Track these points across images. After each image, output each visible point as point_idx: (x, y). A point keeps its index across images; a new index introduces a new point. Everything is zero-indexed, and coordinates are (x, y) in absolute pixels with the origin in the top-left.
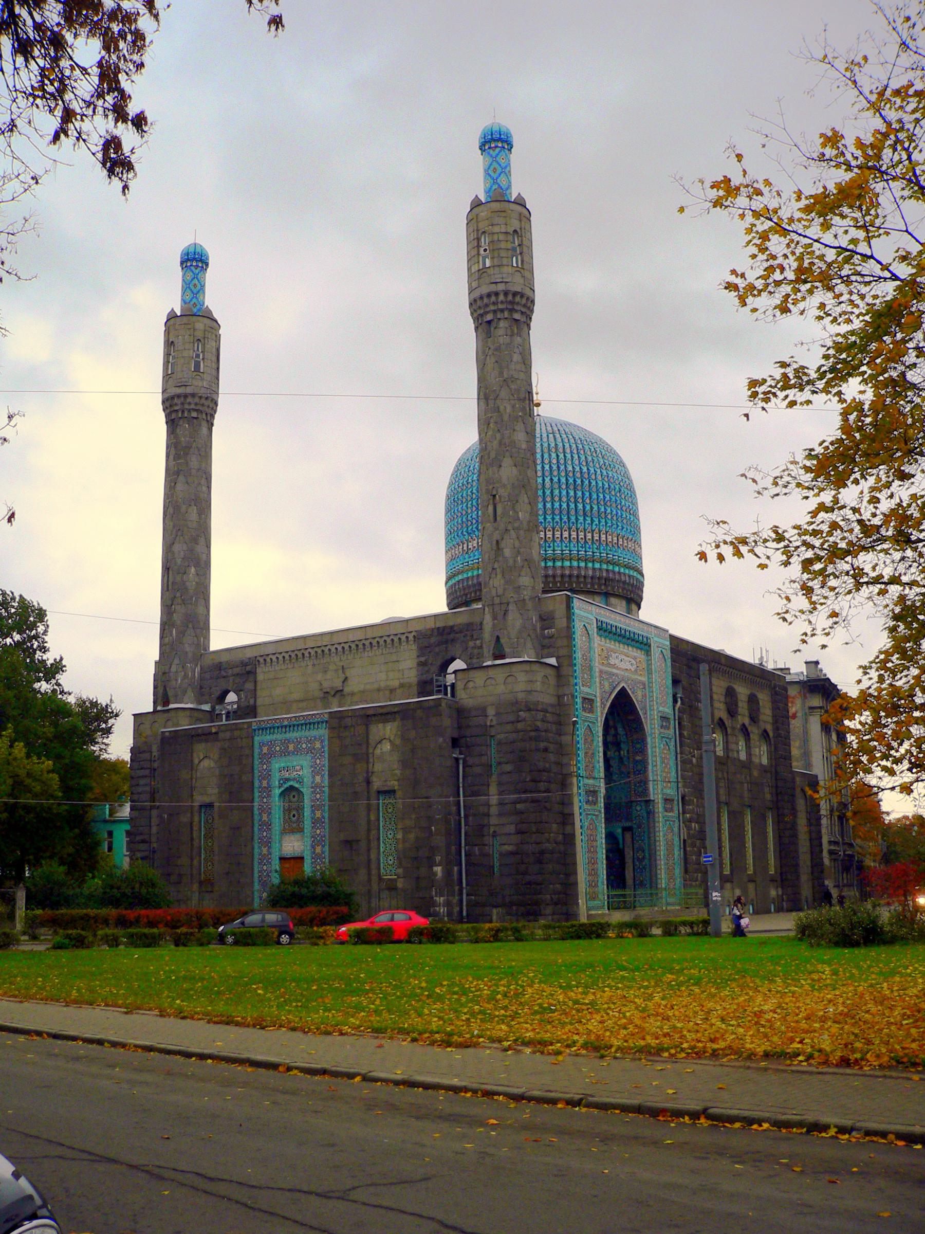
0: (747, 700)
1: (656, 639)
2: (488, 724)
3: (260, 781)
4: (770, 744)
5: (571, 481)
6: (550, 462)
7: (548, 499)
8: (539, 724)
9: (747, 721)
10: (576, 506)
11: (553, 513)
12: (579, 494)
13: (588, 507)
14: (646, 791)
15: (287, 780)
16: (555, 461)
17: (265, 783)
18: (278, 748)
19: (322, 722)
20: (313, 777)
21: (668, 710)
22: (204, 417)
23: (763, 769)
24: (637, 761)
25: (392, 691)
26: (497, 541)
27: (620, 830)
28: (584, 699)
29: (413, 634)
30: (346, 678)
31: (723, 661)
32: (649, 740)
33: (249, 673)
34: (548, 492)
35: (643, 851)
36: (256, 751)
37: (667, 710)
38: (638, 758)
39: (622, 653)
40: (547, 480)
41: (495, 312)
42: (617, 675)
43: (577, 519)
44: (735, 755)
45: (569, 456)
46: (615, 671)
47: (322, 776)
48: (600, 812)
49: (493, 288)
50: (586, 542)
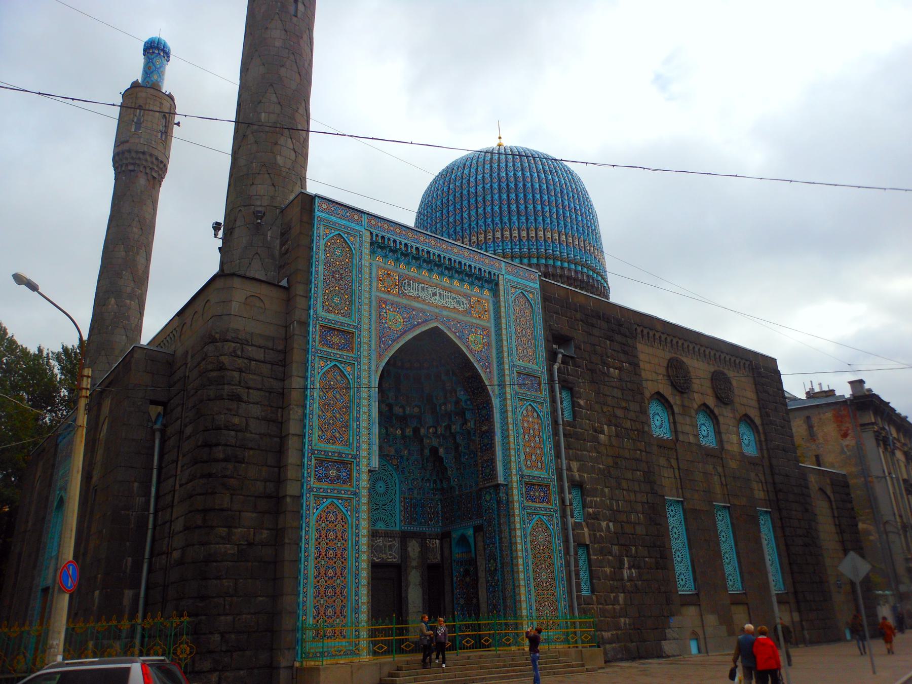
0: (710, 376)
1: (508, 277)
4: (758, 432)
5: (504, 185)
6: (484, 173)
7: (480, 205)
8: (225, 359)
9: (711, 402)
10: (509, 207)
11: (485, 218)
12: (513, 196)
13: (522, 207)
14: (493, 474)
16: (487, 171)
21: (539, 366)
22: (141, 169)
23: (751, 462)
24: (484, 433)
27: (470, 532)
28: (328, 329)
31: (659, 327)
32: (496, 402)
34: (480, 199)
35: (495, 560)
37: (535, 367)
38: (484, 428)
39: (437, 286)
40: (480, 188)
42: (423, 311)
43: (510, 219)
44: (692, 439)
45: (503, 165)
46: (415, 304)
48: (356, 494)
50: (520, 240)
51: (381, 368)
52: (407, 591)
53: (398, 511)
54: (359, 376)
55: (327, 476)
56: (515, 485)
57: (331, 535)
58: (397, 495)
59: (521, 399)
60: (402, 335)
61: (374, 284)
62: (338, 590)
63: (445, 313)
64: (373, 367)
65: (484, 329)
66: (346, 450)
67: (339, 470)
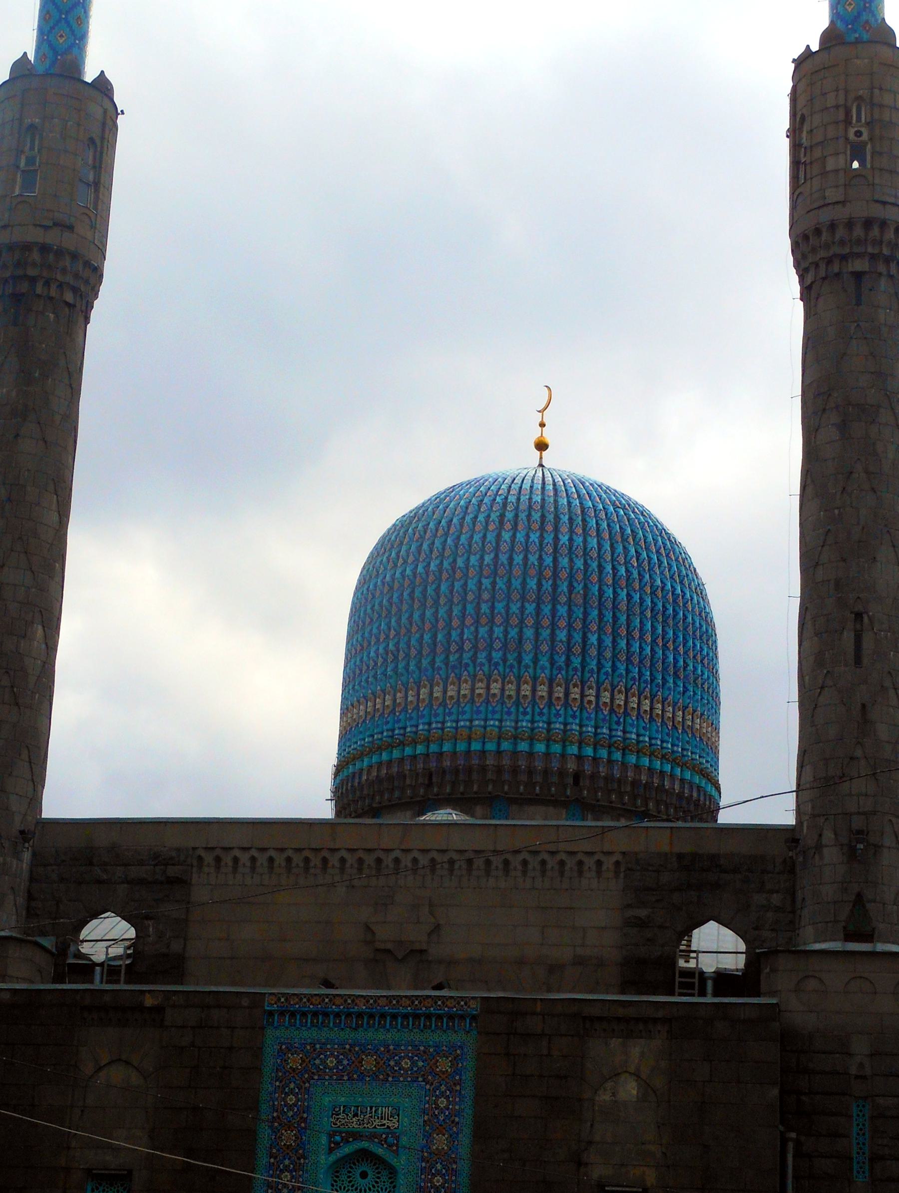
2: (853, 1071)
3: (275, 1131)
15: (356, 1136)
17: (288, 1137)
18: (331, 1062)
19: (462, 1017)
20: (428, 1137)
25: (554, 969)
26: (864, 706)
29: (614, 859)
30: (438, 927)
33: (173, 881)
36: (269, 1062)
41: (873, 257)
47: (453, 1138)
49: (877, 211)
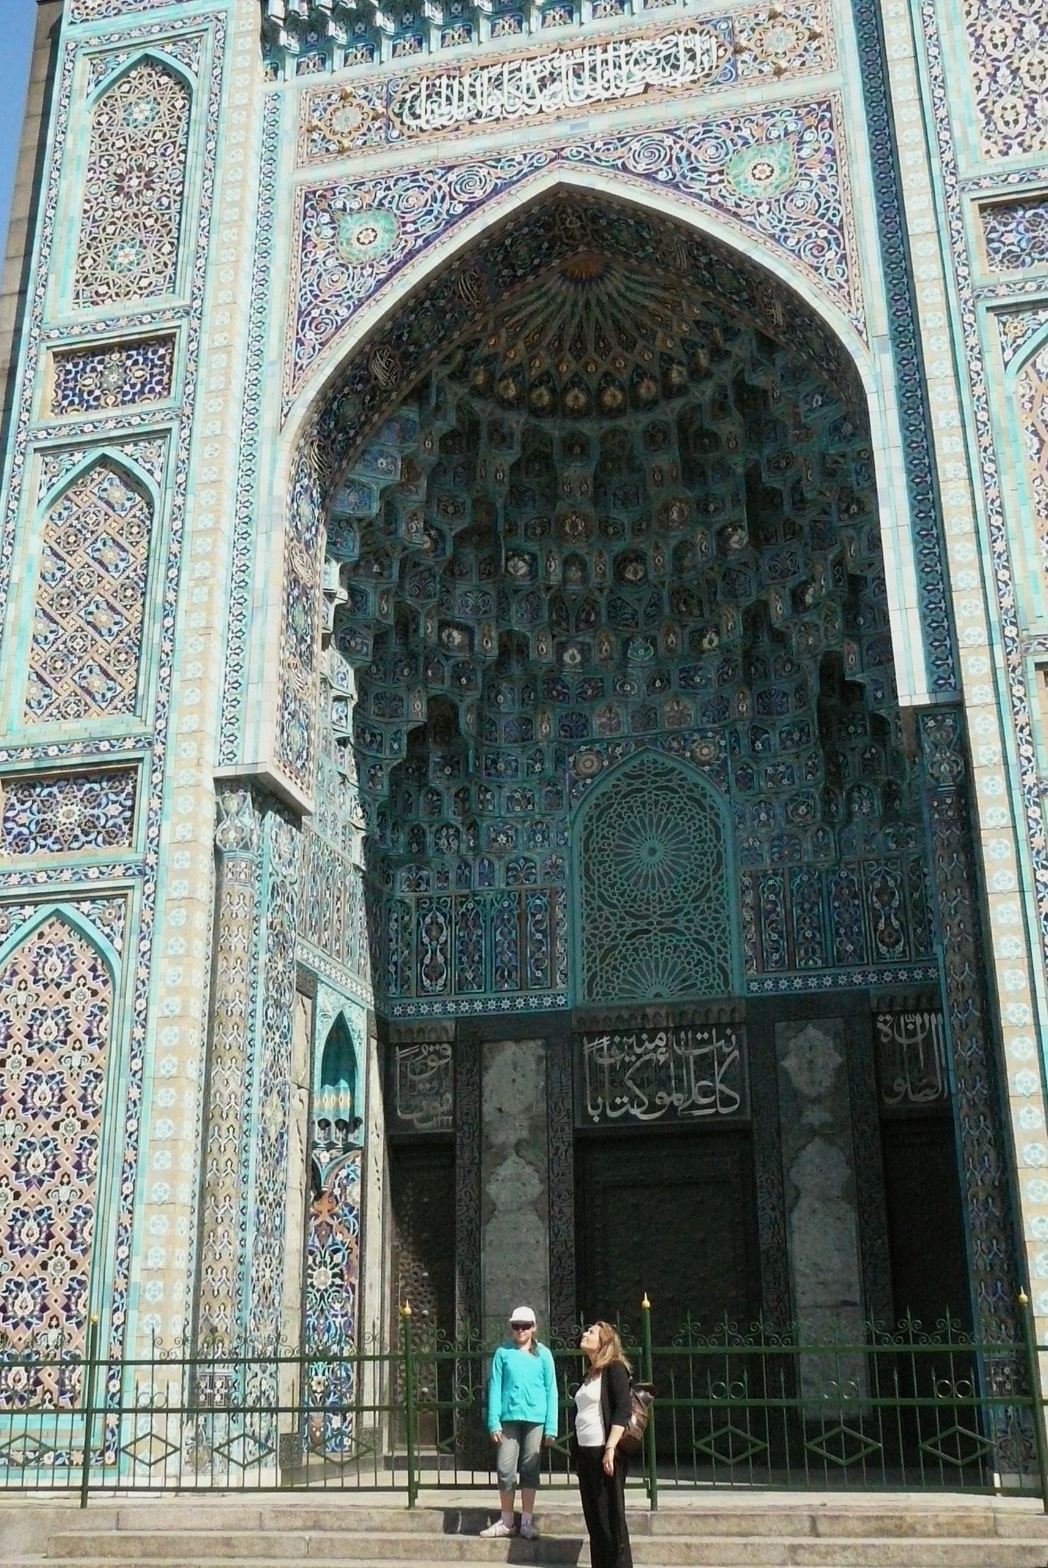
32: (876, 371)
51: (300, 412)
52: (782, 1227)
53: (733, 927)
54: (183, 466)
55: (44, 829)
56: (977, 695)
57: (49, 1030)
58: (729, 871)
59: (1016, 309)
60: (395, 270)
61: (287, 153)
62: (61, 1225)
63: (599, 124)
64: (268, 417)
65: (801, 108)
66: (119, 724)
67: (93, 800)
